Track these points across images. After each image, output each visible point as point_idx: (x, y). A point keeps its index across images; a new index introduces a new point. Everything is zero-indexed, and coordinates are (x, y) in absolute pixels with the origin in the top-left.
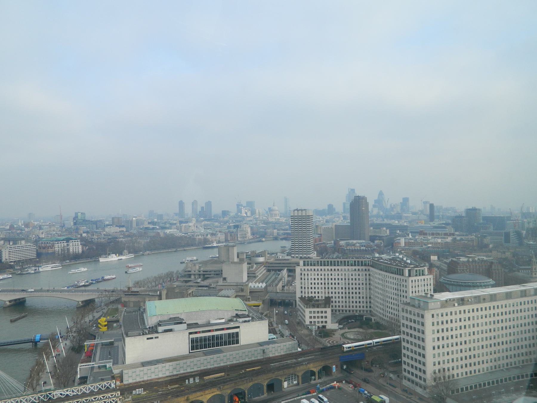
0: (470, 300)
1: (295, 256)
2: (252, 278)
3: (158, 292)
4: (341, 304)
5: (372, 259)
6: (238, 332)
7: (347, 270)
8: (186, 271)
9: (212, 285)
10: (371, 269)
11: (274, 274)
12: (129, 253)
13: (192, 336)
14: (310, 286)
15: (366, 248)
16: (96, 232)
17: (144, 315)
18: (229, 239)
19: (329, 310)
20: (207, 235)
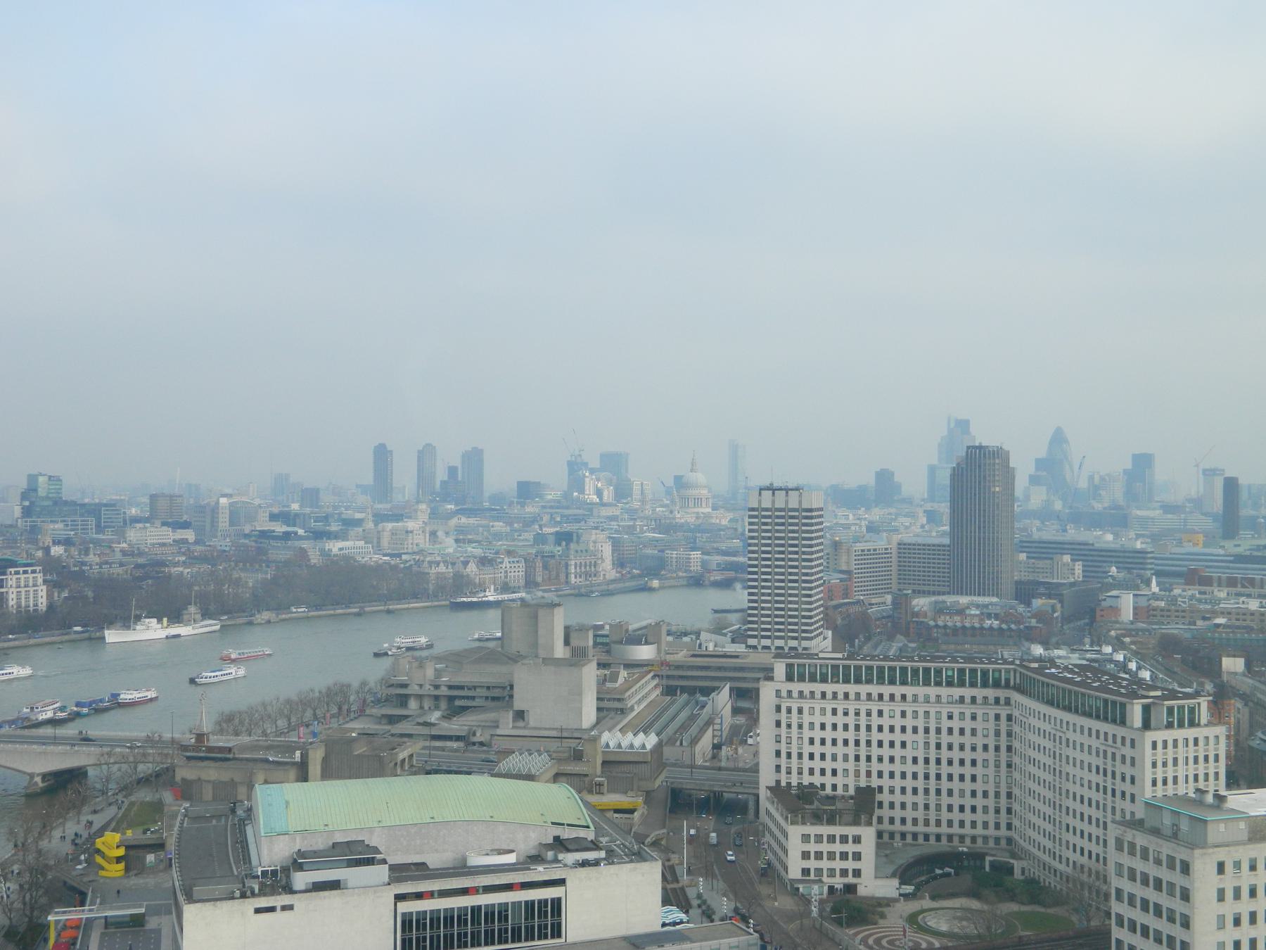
1: (759, 643)
3: (298, 754)
4: (909, 814)
5: (1021, 666)
6: (559, 899)
7: (933, 699)
8: (392, 685)
9: (478, 734)
10: (1016, 697)
11: (687, 704)
12: (206, 615)
13: (404, 907)
14: (807, 749)
15: (1002, 622)
16: (97, 543)
17: (249, 830)
18: (539, 579)
19: (868, 834)
20: (466, 563)
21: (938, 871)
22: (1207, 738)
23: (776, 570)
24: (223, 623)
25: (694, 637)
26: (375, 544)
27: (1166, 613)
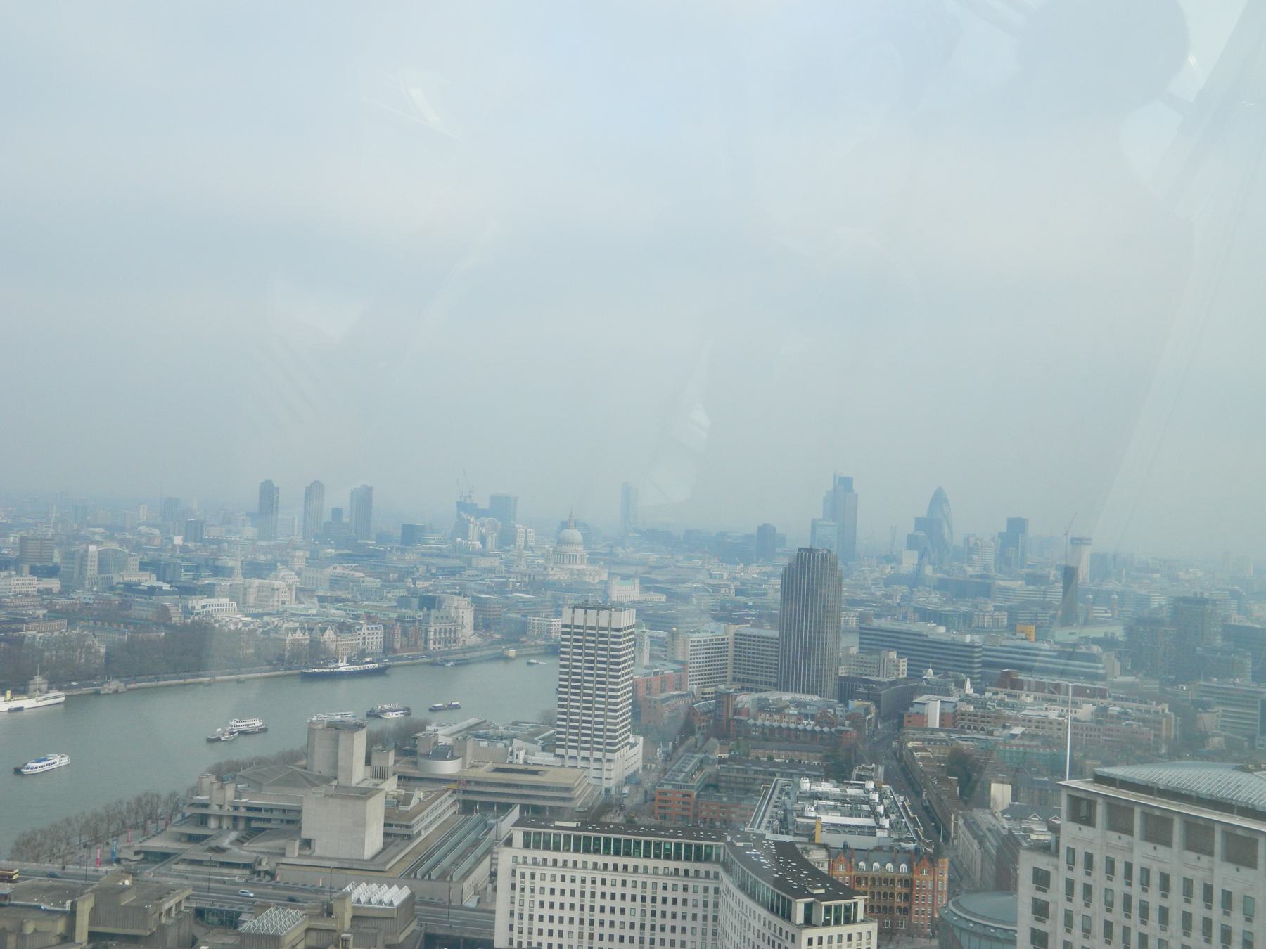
1: (567, 753)
2: (399, 840)
3: (68, 903)
8: (192, 805)
9: (264, 863)
10: (722, 874)
14: (537, 911)
18: (397, 645)
20: (323, 630)
22: (860, 934)
23: (586, 685)
24: (68, 694)
25: (507, 742)
26: (241, 600)
27: (972, 718)
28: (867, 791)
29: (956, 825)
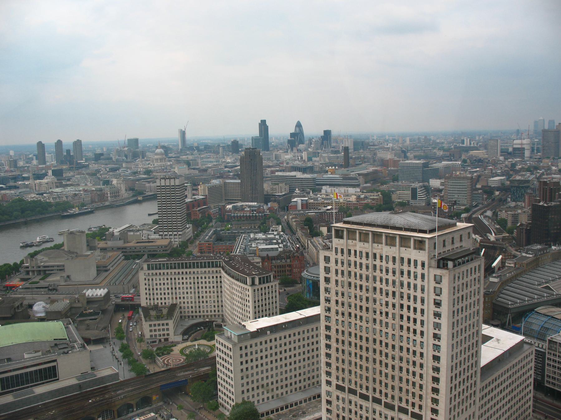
0: (284, 327)
6: (55, 366)
10: (222, 271)
15: (257, 212)
18: (97, 200)
19: (171, 322)
21: (198, 328)
25: (141, 232)
26: (34, 189)
28: (275, 235)
29: (308, 244)
